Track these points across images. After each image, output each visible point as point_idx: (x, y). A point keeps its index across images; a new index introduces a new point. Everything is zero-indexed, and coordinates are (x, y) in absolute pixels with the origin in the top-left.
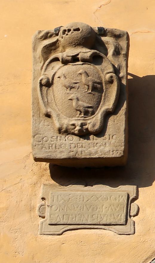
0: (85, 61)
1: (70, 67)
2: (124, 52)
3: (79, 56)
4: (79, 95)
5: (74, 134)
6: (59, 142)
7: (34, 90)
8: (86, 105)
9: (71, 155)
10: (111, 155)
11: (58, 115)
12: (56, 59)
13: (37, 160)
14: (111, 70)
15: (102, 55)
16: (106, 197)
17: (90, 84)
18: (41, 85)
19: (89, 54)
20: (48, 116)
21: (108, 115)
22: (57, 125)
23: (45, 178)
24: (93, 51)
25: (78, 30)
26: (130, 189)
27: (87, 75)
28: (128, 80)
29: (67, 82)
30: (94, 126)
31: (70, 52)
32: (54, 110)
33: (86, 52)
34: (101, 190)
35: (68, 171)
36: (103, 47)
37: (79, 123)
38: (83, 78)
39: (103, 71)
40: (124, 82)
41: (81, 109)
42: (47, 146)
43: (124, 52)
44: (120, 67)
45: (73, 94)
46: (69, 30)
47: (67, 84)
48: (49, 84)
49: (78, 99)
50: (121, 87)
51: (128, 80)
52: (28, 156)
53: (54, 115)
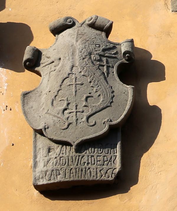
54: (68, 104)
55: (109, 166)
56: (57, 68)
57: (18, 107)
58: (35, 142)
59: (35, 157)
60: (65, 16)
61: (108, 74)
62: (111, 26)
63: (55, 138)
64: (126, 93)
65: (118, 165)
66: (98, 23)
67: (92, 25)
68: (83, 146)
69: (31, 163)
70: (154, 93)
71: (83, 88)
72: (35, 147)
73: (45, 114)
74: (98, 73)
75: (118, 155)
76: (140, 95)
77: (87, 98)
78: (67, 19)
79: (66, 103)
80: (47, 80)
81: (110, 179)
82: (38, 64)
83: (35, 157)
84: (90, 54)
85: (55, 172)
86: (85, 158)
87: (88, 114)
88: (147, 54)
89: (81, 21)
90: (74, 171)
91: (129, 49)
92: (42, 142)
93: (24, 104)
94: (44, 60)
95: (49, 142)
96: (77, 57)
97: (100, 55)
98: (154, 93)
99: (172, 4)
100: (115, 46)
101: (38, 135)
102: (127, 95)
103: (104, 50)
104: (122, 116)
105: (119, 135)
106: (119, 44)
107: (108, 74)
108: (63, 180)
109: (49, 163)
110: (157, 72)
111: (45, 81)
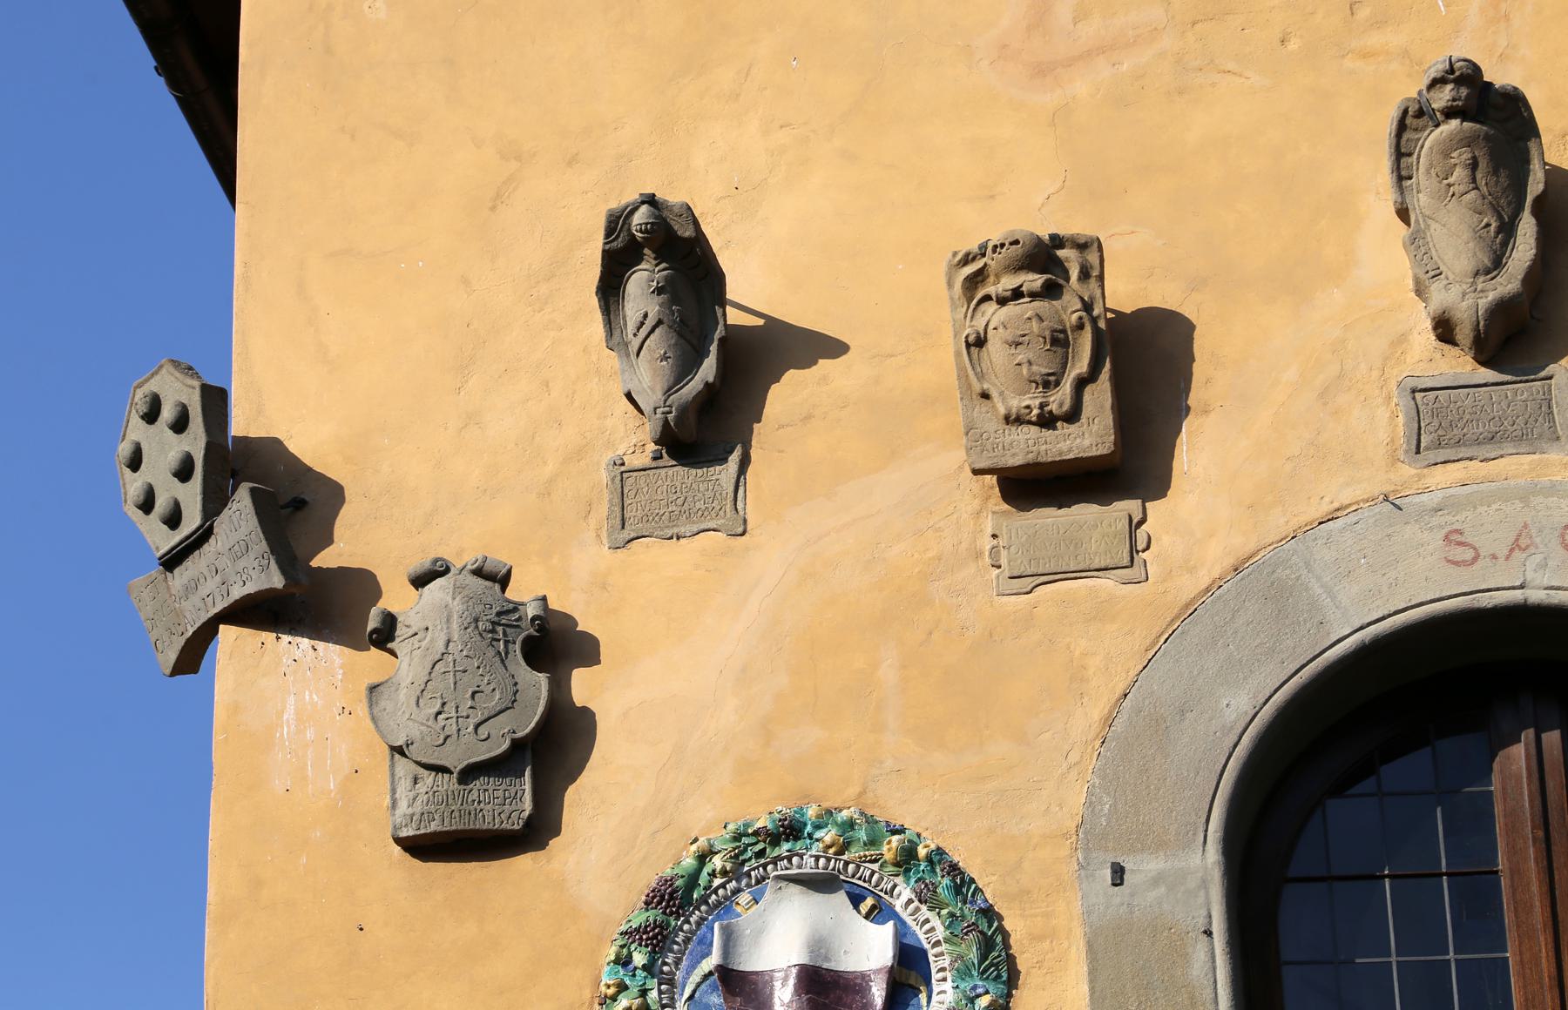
0: (1034, 295)
1: (1011, 309)
2: (1095, 273)
3: (1024, 289)
4: (1031, 356)
5: (1030, 422)
6: (1008, 440)
7: (958, 354)
8: (1045, 371)
9: (1030, 458)
10: (1094, 452)
11: (1001, 394)
12: (987, 298)
13: (976, 472)
14: (1079, 306)
15: (1061, 282)
16: (1092, 523)
17: (1047, 333)
18: (968, 345)
19: (1039, 283)
20: (985, 396)
21: (1081, 384)
22: (1002, 411)
23: (992, 501)
24: (1045, 277)
25: (1016, 242)
26: (1131, 506)
27: (1041, 319)
28: (1108, 321)
29: (1009, 335)
30: (1061, 405)
31: (1008, 283)
32: (994, 385)
33: (1034, 281)
34: (1084, 513)
35: (1027, 487)
36: (1059, 267)
37: (1037, 402)
38: (1035, 324)
39: (1065, 309)
40: (1102, 324)
41: (1037, 378)
42: (989, 447)
43: (1095, 273)
44: (1092, 298)
45: (1022, 355)
46: (1002, 245)
47: (1010, 339)
48: (980, 342)
49: (1030, 363)
50: (1097, 332)
51: (1108, 321)
52: (961, 468)
53: (994, 394)
54: (444, 704)
55: (514, 807)
56: (424, 644)
57: (362, 710)
58: (392, 766)
59: (394, 791)
60: (433, 556)
61: (507, 653)
62: (509, 572)
63: (424, 760)
64: (537, 684)
65: (528, 805)
66: (488, 567)
67: (478, 572)
68: (470, 773)
69: (387, 801)
70: (583, 686)
71: (466, 678)
72: (393, 775)
73: (408, 722)
74: (491, 652)
75: (528, 787)
76: (560, 688)
77: (474, 693)
78: (437, 560)
79: (439, 702)
80: (406, 665)
81: (516, 827)
82: (391, 638)
83: (394, 791)
84: (476, 620)
85: (426, 816)
86: (475, 792)
87: (477, 720)
88: (569, 620)
89: (459, 566)
90: (456, 814)
91: (539, 612)
92: (404, 767)
93: (371, 704)
94: (401, 631)
95: (414, 766)
96: (455, 626)
97: (493, 623)
98: (583, 686)
99: (609, 536)
100: (516, 607)
101: (397, 756)
102: (539, 689)
103: (499, 614)
104: (533, 725)
105: (529, 755)
106: (522, 604)
107: (507, 653)
108: (439, 829)
109: (418, 803)
110: (586, 650)
111: (404, 666)
